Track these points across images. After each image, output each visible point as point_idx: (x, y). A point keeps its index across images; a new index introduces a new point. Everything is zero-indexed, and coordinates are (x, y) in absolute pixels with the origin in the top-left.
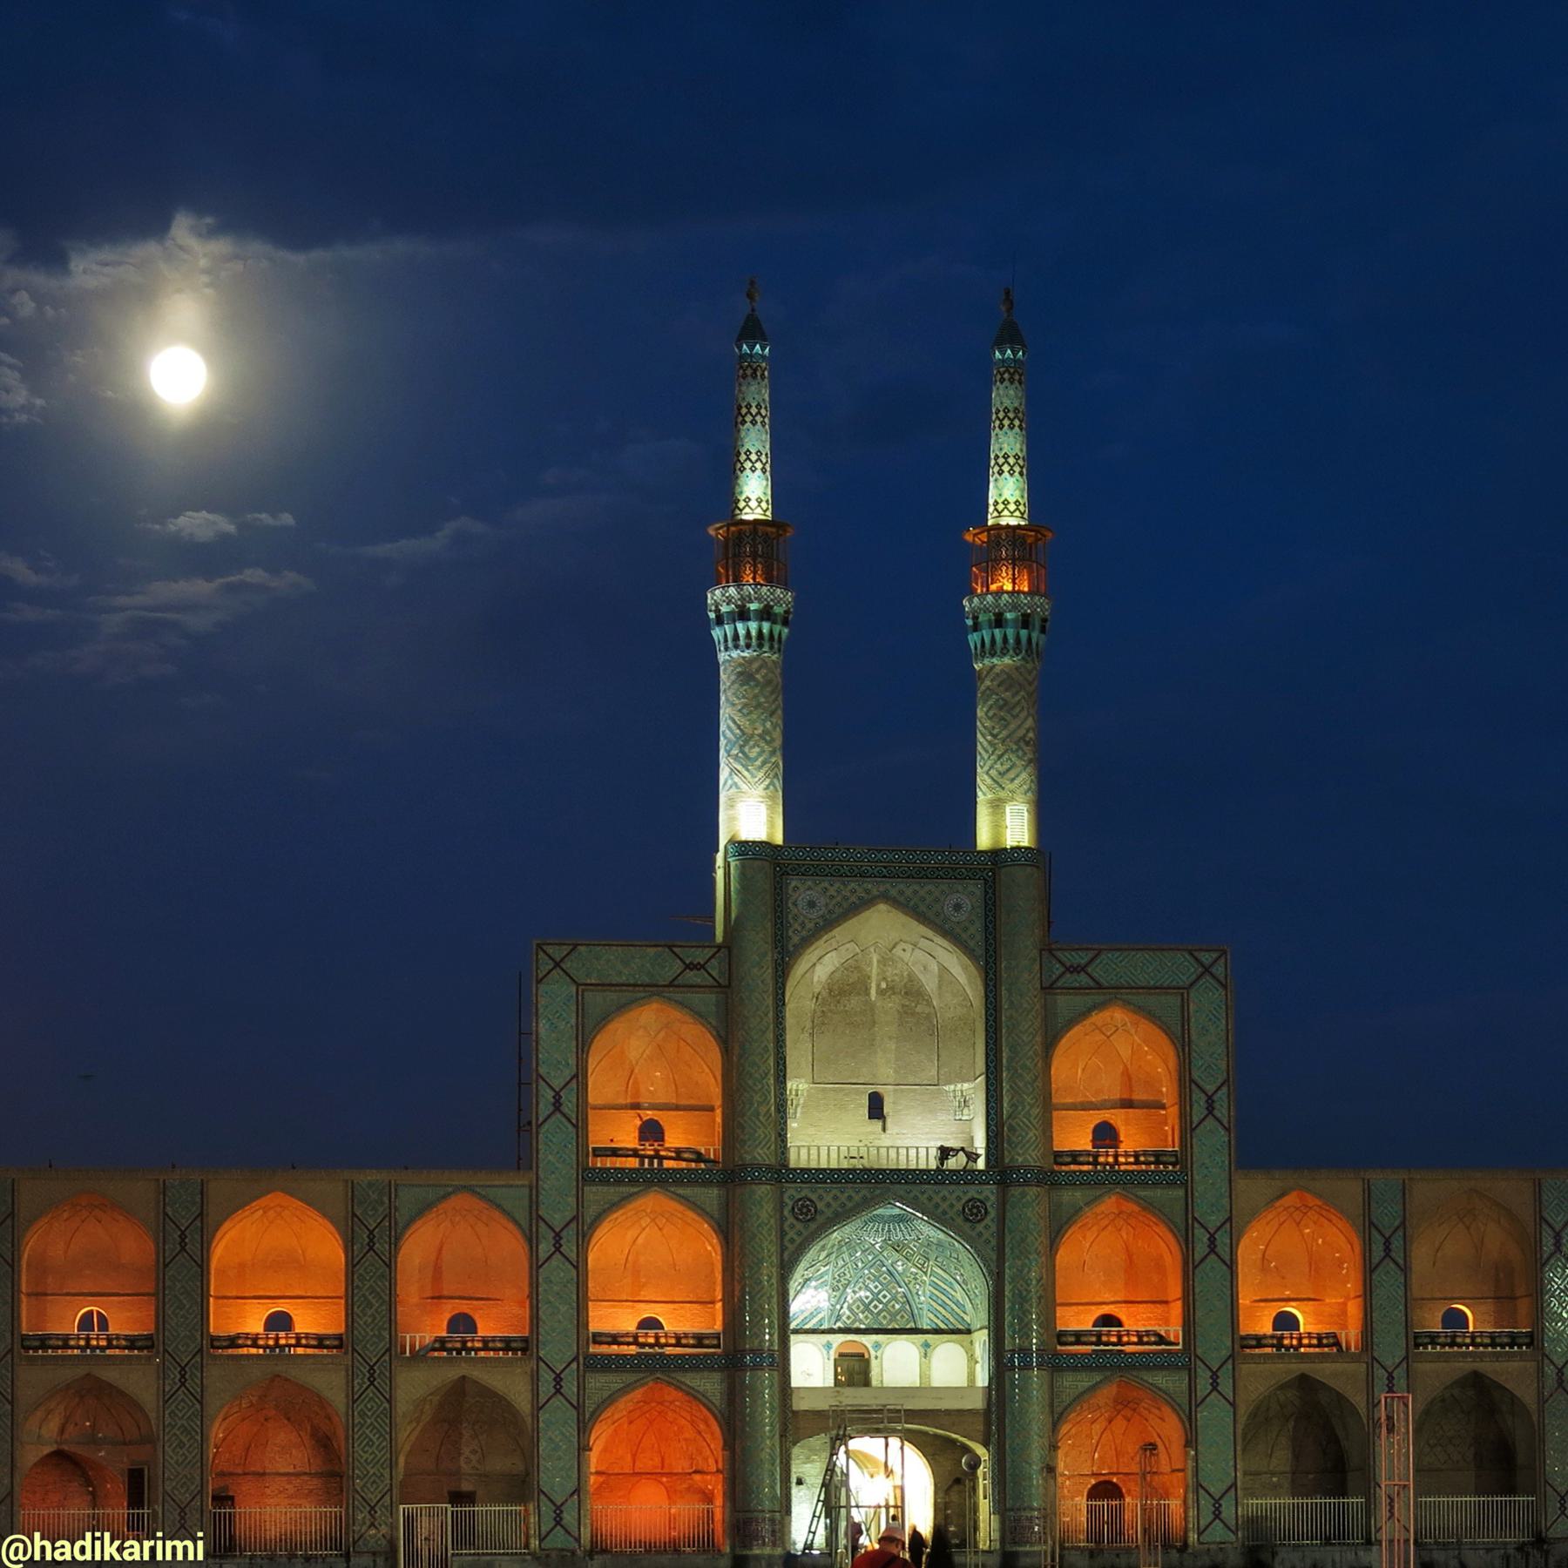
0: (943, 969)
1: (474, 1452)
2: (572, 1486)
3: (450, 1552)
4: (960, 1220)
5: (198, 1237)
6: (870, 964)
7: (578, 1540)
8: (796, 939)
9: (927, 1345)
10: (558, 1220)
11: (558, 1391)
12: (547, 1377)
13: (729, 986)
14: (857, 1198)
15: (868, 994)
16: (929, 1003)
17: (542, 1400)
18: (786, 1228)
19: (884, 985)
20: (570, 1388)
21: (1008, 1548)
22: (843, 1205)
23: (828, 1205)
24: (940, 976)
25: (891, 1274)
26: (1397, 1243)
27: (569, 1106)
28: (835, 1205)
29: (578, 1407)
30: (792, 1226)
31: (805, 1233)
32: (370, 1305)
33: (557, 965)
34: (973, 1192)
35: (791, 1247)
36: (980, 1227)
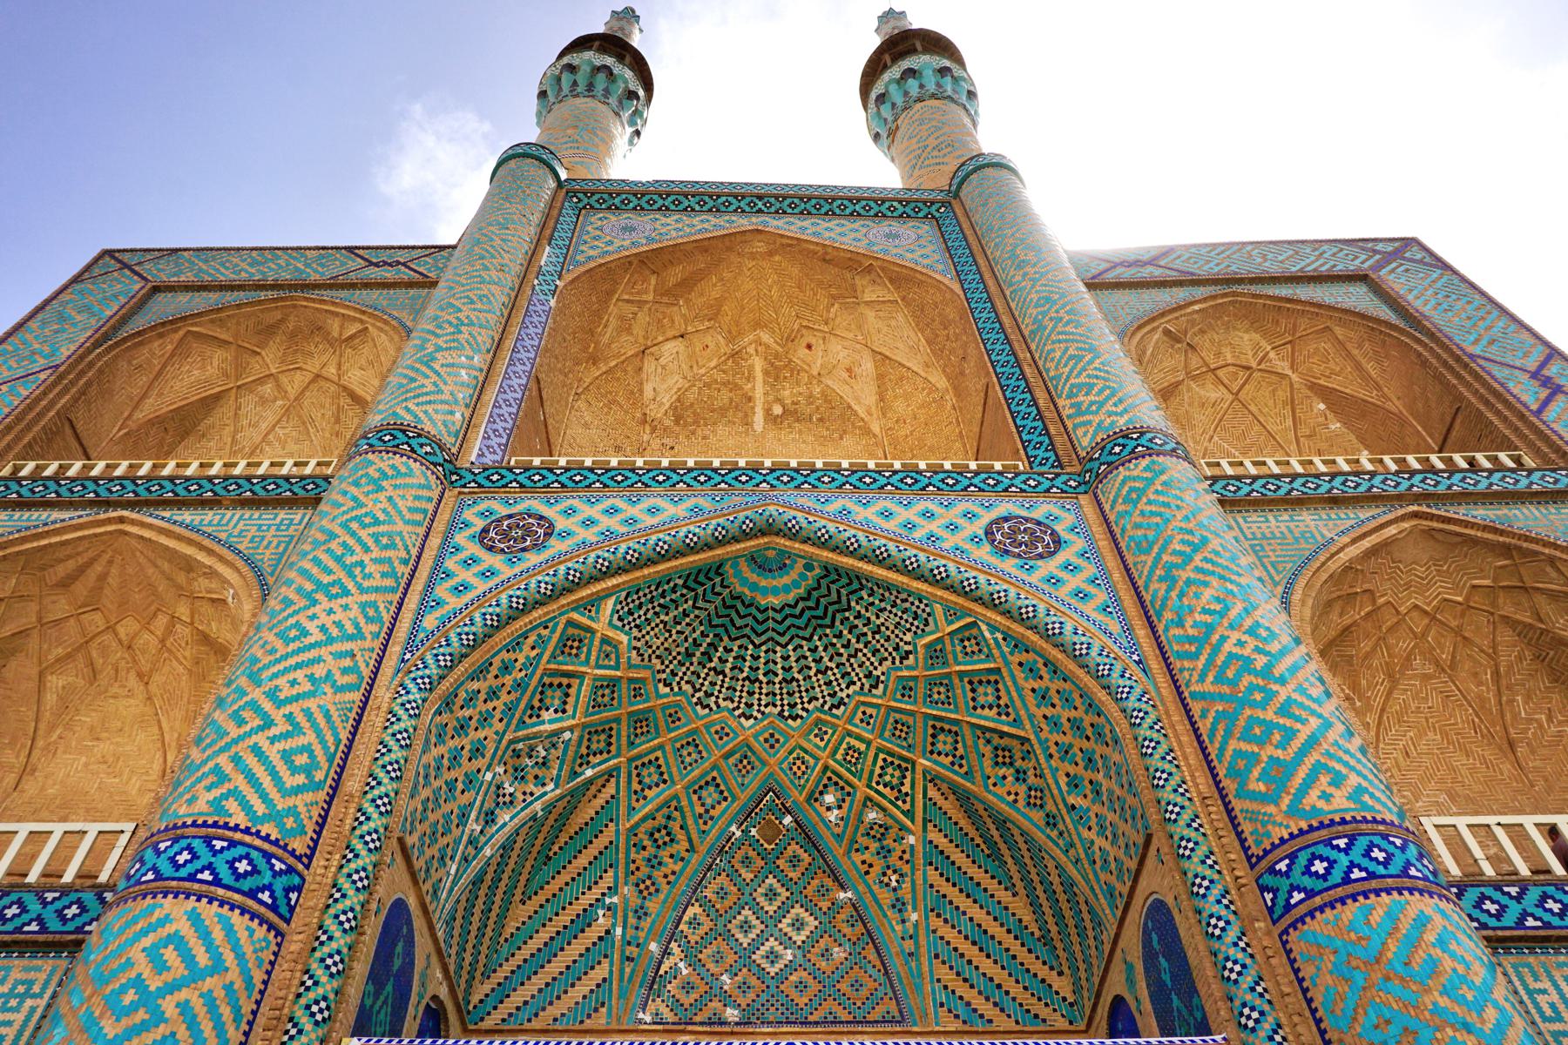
0: (882, 359)
4: (984, 553)
6: (750, 378)
8: (592, 253)
15: (747, 423)
16: (867, 431)
18: (450, 564)
19: (778, 410)
22: (631, 521)
23: (588, 523)
24: (880, 377)
25: (811, 842)
30: (468, 563)
31: (506, 572)
34: (1005, 507)
35: (454, 602)
36: (1051, 566)
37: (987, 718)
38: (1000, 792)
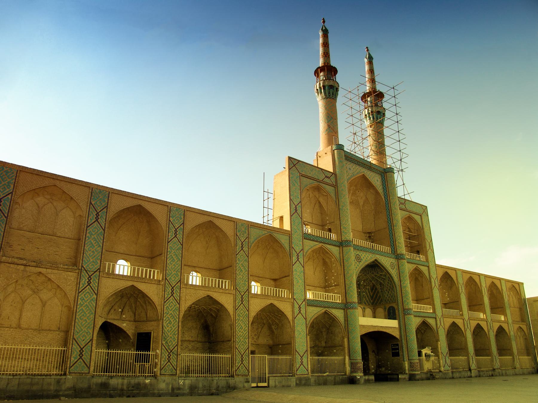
1: (255, 335)
2: (305, 349)
3: (267, 375)
5: (182, 233)
7: (308, 371)
9: (364, 308)
10: (298, 249)
11: (300, 312)
12: (296, 306)
13: (337, 185)
14: (370, 257)
17: (296, 315)
20: (303, 311)
21: (412, 373)
26: (463, 288)
27: (299, 211)
28: (365, 258)
29: (306, 319)
31: (360, 266)
32: (241, 271)
33: (294, 165)
37: (382, 281)
38: (378, 287)
